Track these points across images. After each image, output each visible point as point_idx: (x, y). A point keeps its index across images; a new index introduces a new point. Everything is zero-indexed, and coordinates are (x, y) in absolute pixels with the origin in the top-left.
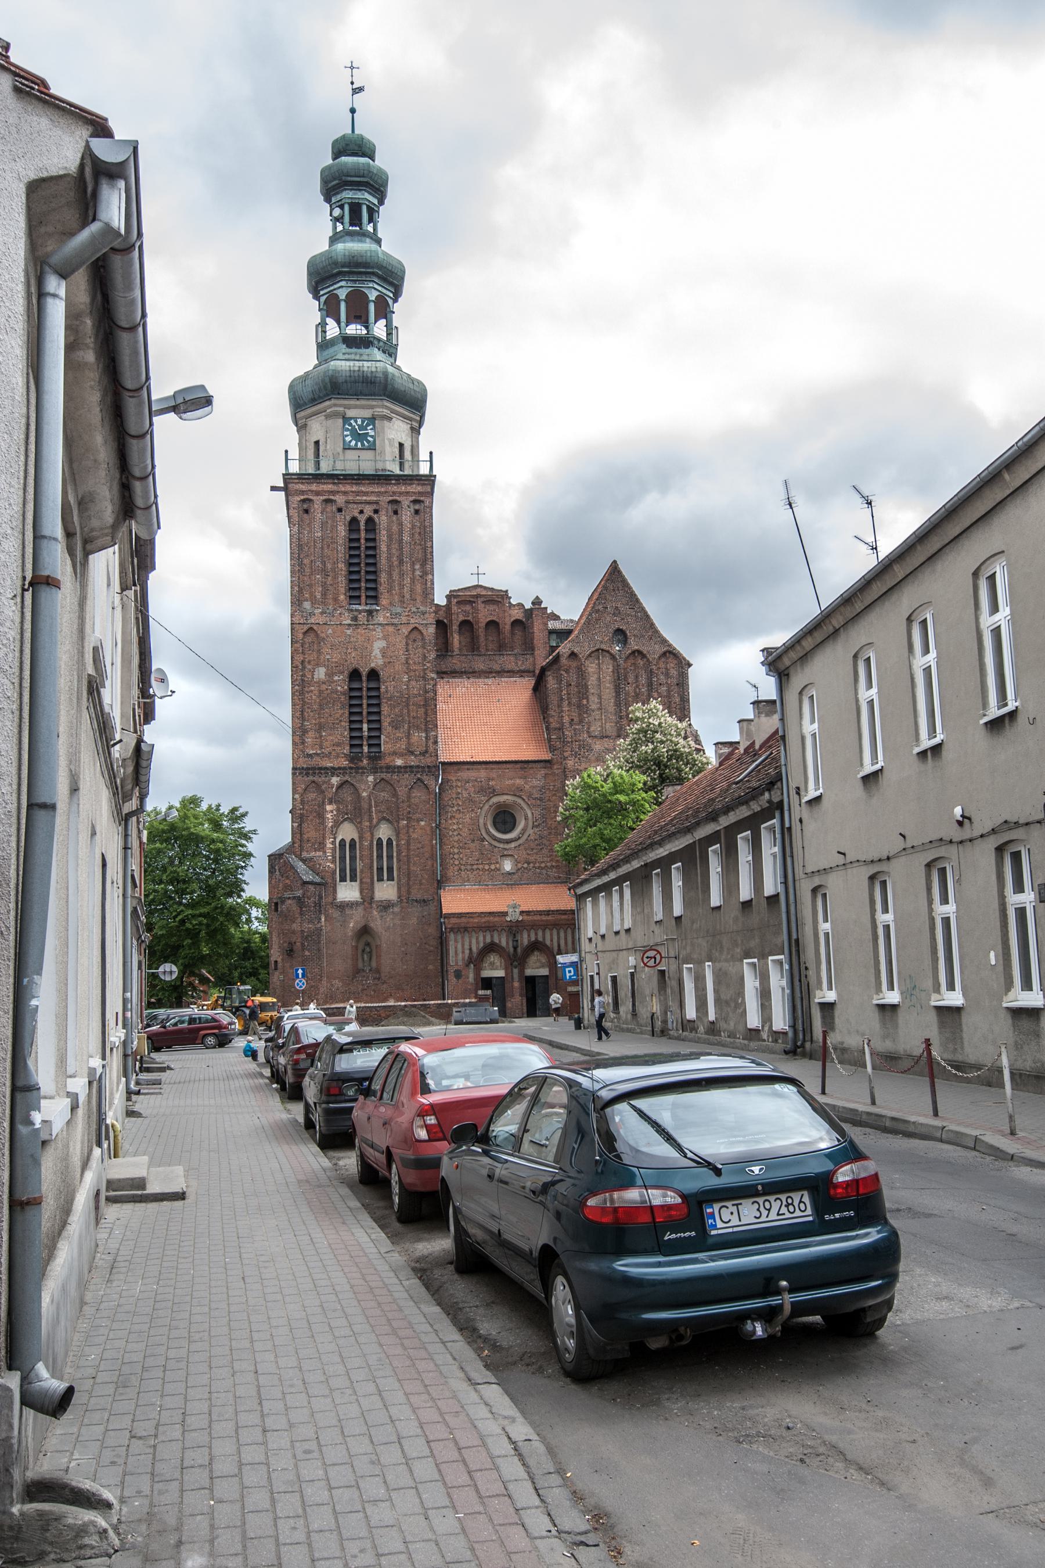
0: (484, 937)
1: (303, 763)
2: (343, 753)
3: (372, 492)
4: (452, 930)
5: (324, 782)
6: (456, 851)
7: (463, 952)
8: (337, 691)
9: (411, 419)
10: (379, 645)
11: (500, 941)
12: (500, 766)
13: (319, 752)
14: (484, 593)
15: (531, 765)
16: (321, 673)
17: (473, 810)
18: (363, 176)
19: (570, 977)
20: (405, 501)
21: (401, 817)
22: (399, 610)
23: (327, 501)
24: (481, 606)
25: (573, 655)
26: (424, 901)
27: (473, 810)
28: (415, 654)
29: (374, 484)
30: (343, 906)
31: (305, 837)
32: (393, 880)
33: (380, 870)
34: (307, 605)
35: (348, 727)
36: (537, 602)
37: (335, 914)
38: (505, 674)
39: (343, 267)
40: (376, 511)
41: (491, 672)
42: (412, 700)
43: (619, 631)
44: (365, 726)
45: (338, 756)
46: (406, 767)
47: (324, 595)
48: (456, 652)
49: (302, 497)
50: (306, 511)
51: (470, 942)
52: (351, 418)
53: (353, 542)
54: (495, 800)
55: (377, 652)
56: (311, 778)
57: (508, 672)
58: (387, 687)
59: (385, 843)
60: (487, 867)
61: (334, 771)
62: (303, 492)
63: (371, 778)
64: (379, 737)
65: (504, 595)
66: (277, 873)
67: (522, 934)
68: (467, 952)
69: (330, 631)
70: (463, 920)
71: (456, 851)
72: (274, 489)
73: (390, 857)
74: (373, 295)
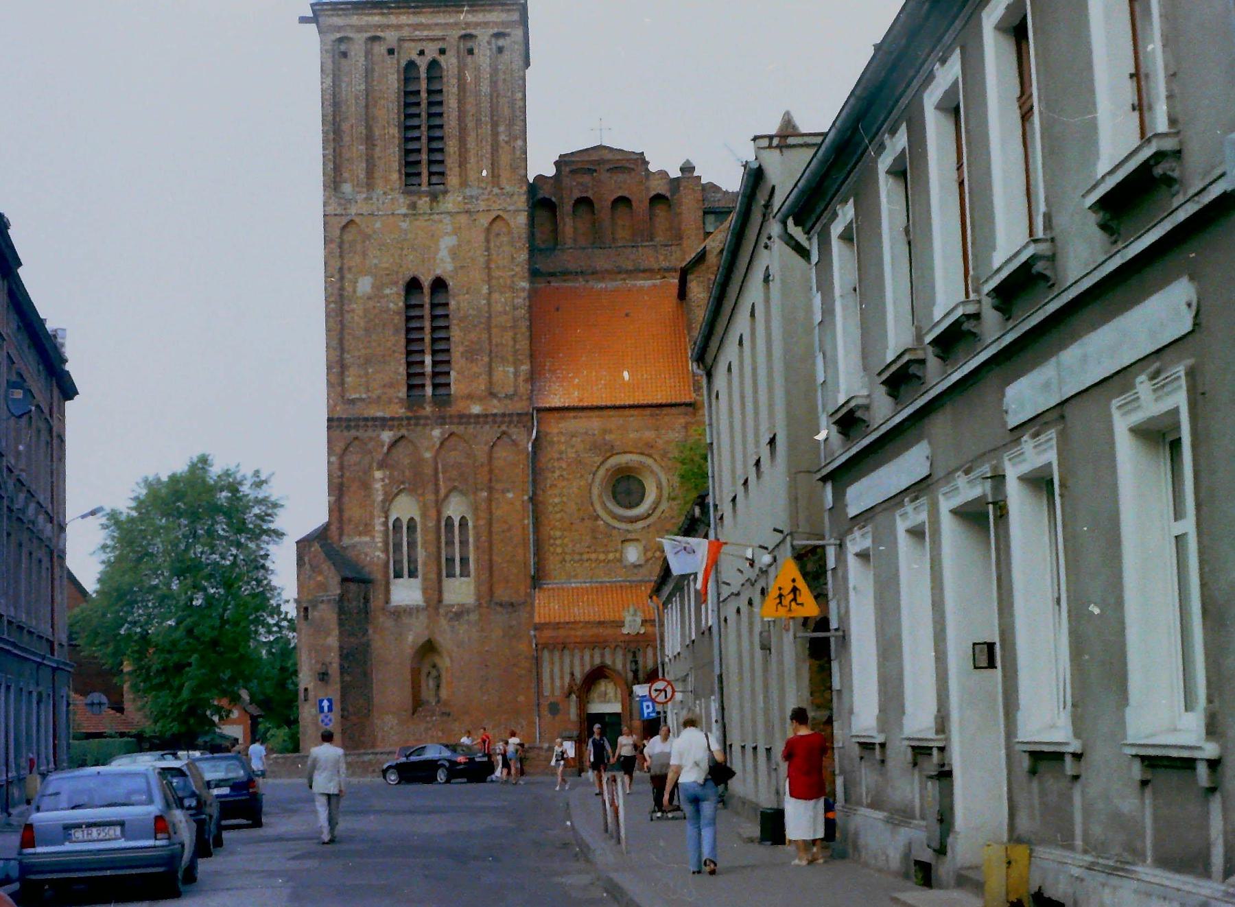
0: (592, 657)
1: (340, 412)
2: (397, 397)
3: (437, 25)
4: (545, 646)
5: (371, 439)
6: (558, 534)
7: (562, 678)
8: (388, 309)
10: (447, 242)
11: (614, 662)
12: (621, 412)
13: (364, 396)
14: (609, 156)
15: (665, 410)
16: (365, 285)
17: (582, 476)
19: (648, 713)
20: (483, 35)
21: (479, 487)
22: (475, 192)
23: (375, 39)
24: (604, 176)
26: (512, 605)
27: (582, 476)
28: (498, 255)
29: (438, 12)
30: (400, 613)
31: (347, 515)
32: (468, 576)
33: (450, 561)
34: (347, 188)
35: (403, 361)
36: (687, 169)
37: (389, 623)
38: (641, 275)
40: (442, 52)
41: (619, 273)
42: (494, 322)
44: (428, 360)
45: (390, 402)
46: (486, 416)
47: (370, 173)
48: (570, 243)
50: (345, 55)
51: (572, 662)
53: (409, 98)
54: (613, 461)
55: (443, 253)
56: (353, 433)
57: (644, 271)
58: (458, 303)
59: (457, 524)
60: (602, 557)
61: (384, 423)
62: (339, 29)
63: (437, 433)
64: (448, 373)
65: (640, 160)
66: (307, 566)
67: (645, 654)
68: (567, 679)
69: (378, 225)
70: (562, 633)
71: (558, 534)
72: (303, 20)
73: (464, 543)
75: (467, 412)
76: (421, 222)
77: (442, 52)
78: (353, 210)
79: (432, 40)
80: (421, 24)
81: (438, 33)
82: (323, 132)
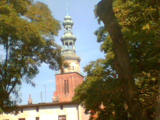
9: (75, 62)
20: (72, 76)
40: (68, 78)
62: (57, 77)
74: (69, 43)
76: (66, 98)
79: (67, 77)
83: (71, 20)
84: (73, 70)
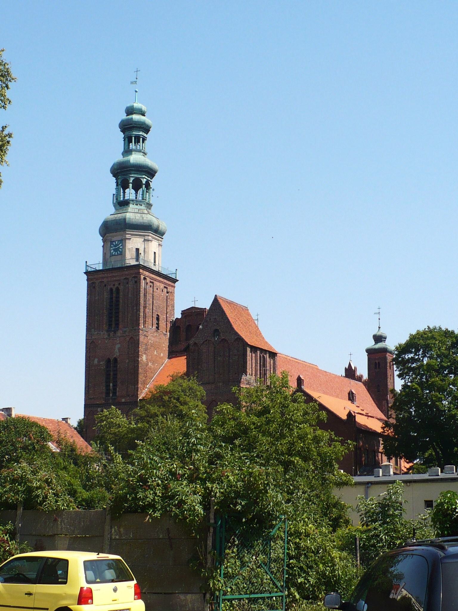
10: (118, 346)
18: (131, 124)
25: (195, 344)
39: (118, 170)
40: (119, 284)
43: (216, 331)
49: (92, 282)
52: (113, 241)
55: (117, 350)
62: (92, 279)
69: (100, 342)
75: (120, 401)
77: (119, 284)
78: (93, 338)
80: (113, 276)
81: (118, 278)
82: (87, 313)
83: (144, 115)
84: (137, 259)
